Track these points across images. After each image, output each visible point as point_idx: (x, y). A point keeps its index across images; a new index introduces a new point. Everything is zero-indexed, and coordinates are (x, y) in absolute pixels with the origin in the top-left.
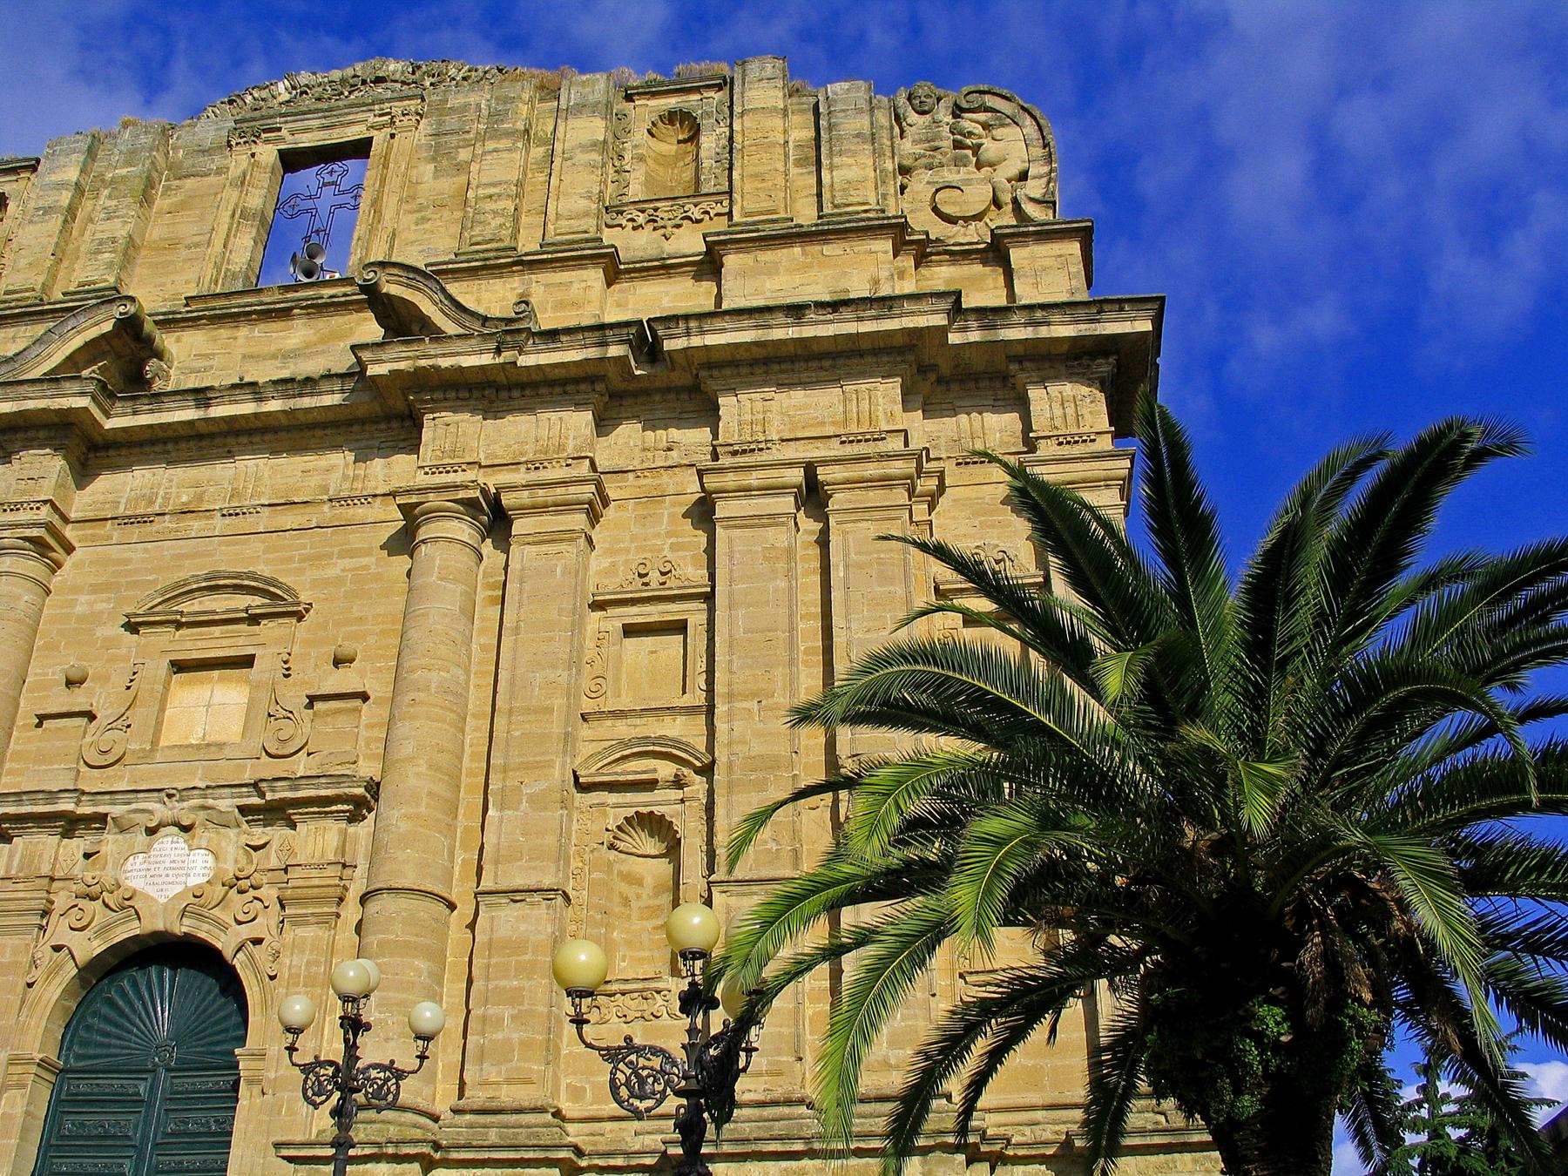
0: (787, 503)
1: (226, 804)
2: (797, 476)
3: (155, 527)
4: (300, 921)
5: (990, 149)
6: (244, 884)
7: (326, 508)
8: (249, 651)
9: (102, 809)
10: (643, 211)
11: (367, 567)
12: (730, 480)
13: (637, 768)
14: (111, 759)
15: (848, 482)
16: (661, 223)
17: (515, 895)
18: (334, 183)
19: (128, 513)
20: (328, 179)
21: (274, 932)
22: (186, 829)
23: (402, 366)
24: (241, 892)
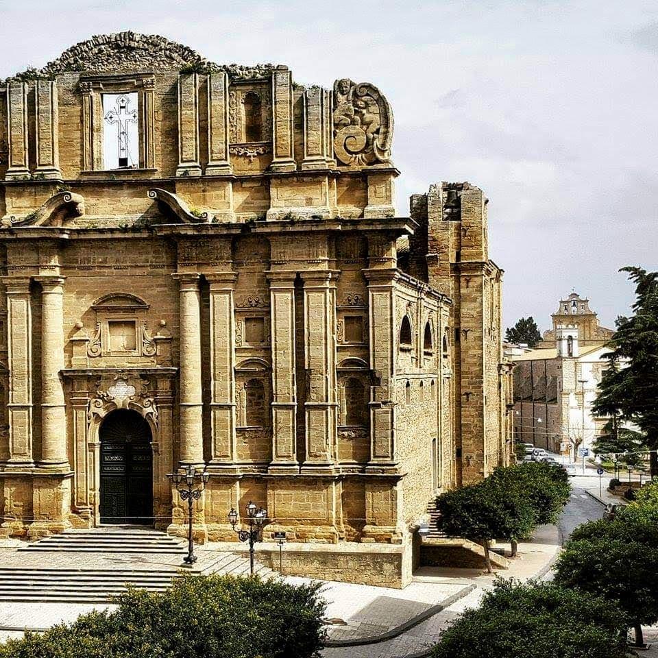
0: (291, 285)
1: (136, 374)
2: (294, 276)
3: (93, 271)
4: (163, 407)
5: (368, 117)
6: (145, 396)
7: (149, 268)
8: (134, 320)
9: (100, 374)
10: (242, 148)
11: (165, 291)
12: (274, 277)
13: (251, 368)
14: (97, 354)
15: (309, 278)
16: (249, 154)
17: (221, 407)
18: (124, 107)
19: (82, 265)
20: (123, 105)
21: (155, 410)
22: (126, 381)
23: (169, 232)
24: (145, 398)
